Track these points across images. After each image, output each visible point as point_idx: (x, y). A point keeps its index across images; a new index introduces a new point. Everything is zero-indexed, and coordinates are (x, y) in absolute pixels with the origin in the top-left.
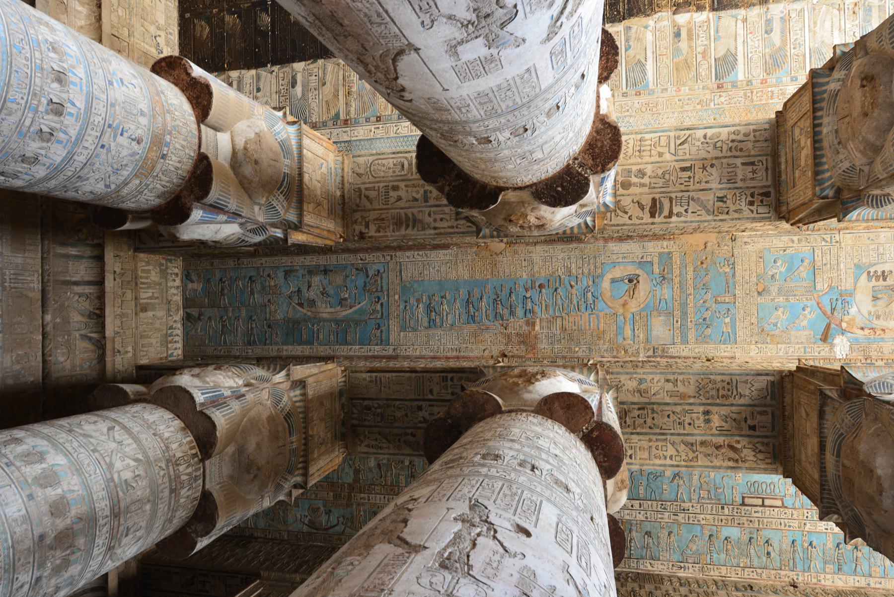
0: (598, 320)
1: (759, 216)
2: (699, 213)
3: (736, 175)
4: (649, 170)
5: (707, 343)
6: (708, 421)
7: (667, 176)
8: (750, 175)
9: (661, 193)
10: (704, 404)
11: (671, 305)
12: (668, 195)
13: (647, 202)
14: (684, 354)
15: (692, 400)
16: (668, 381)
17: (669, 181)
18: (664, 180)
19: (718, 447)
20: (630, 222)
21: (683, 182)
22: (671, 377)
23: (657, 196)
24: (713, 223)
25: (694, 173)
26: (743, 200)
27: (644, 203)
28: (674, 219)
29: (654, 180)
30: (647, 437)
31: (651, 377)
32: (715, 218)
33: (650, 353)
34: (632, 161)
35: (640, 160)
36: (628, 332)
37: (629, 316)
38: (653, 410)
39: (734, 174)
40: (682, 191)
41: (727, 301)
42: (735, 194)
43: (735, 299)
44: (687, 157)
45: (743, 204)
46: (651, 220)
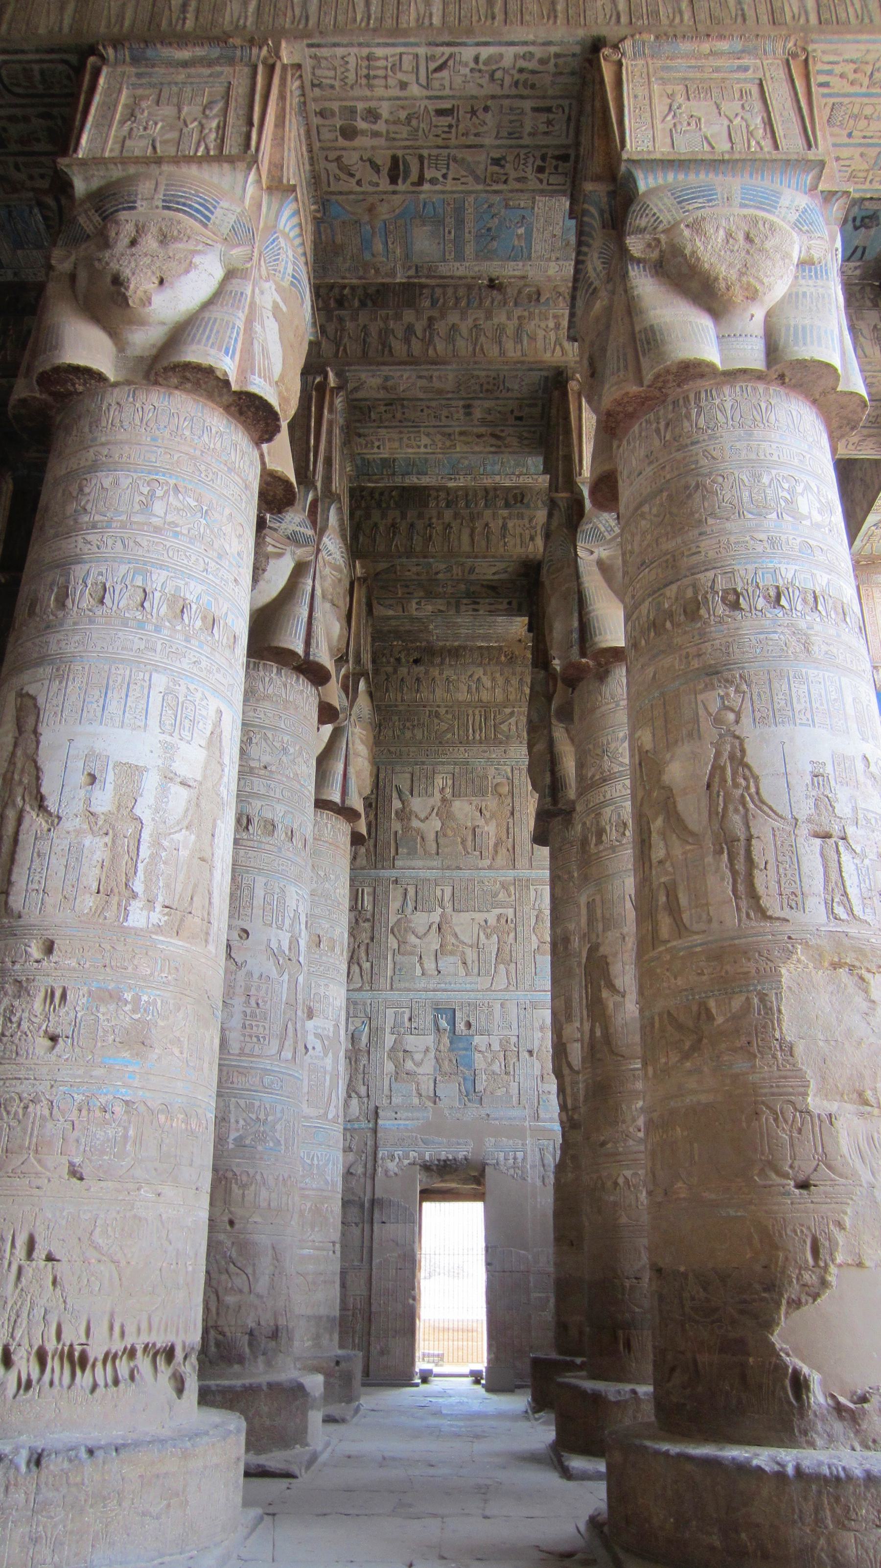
0: (332, 231)
1: (550, 187)
2: (463, 180)
3: (522, 126)
4: (385, 109)
5: (491, 259)
6: (468, 414)
7: (414, 123)
8: (543, 128)
9: (406, 147)
10: (463, 399)
11: (441, 211)
12: (417, 151)
13: (383, 159)
14: (458, 274)
15: (450, 396)
16: (420, 377)
17: (417, 130)
18: (409, 128)
19: (479, 436)
20: (358, 189)
21: (440, 132)
22: (425, 373)
23: (400, 153)
24: (484, 195)
25: (458, 119)
26: (530, 165)
27: (379, 163)
28: (426, 187)
29: (392, 128)
30: (397, 430)
31: (399, 374)
32: (488, 188)
33: (412, 272)
34: (357, 92)
35: (368, 93)
36: (379, 247)
37: (379, 225)
38: (403, 406)
39: (518, 124)
40: (438, 147)
41: (522, 205)
42: (518, 155)
43: (534, 203)
44: (447, 92)
45: (529, 170)
46: (391, 188)
